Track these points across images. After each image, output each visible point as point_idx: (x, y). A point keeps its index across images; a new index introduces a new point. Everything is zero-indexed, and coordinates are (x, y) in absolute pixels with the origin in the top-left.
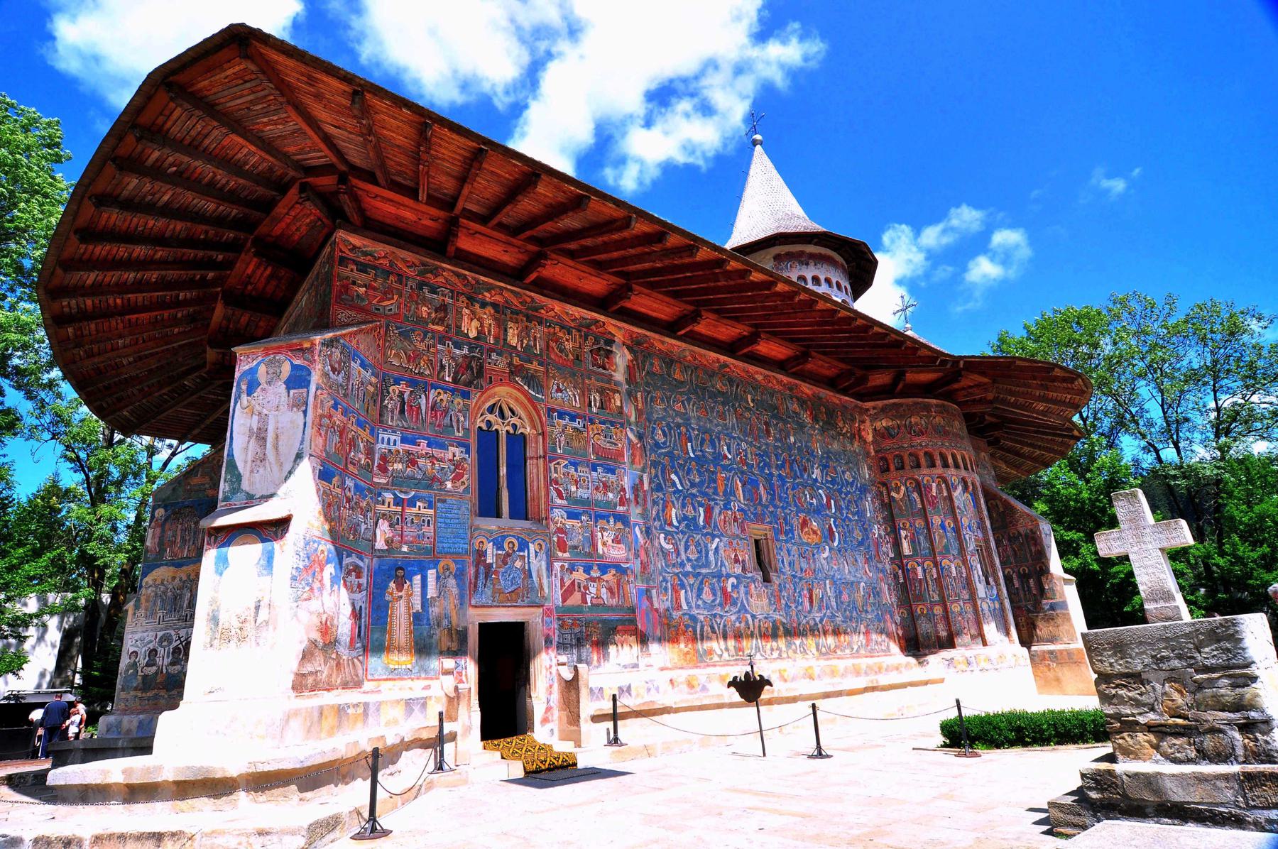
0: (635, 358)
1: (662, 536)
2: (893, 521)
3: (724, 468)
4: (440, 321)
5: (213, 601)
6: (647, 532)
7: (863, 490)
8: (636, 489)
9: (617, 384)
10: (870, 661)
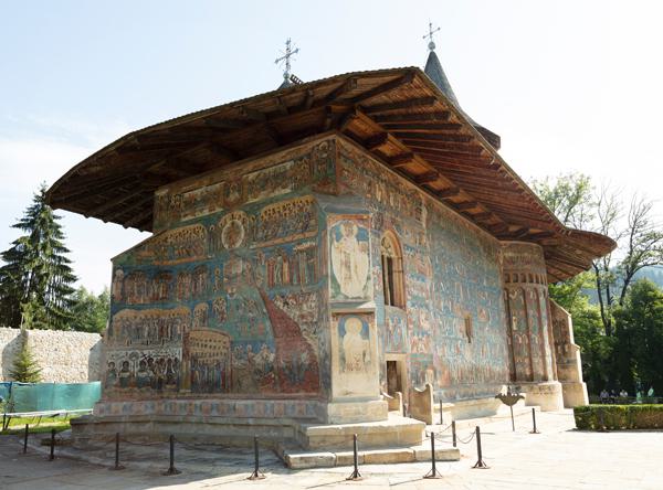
4: (369, 192)
5: (341, 350)
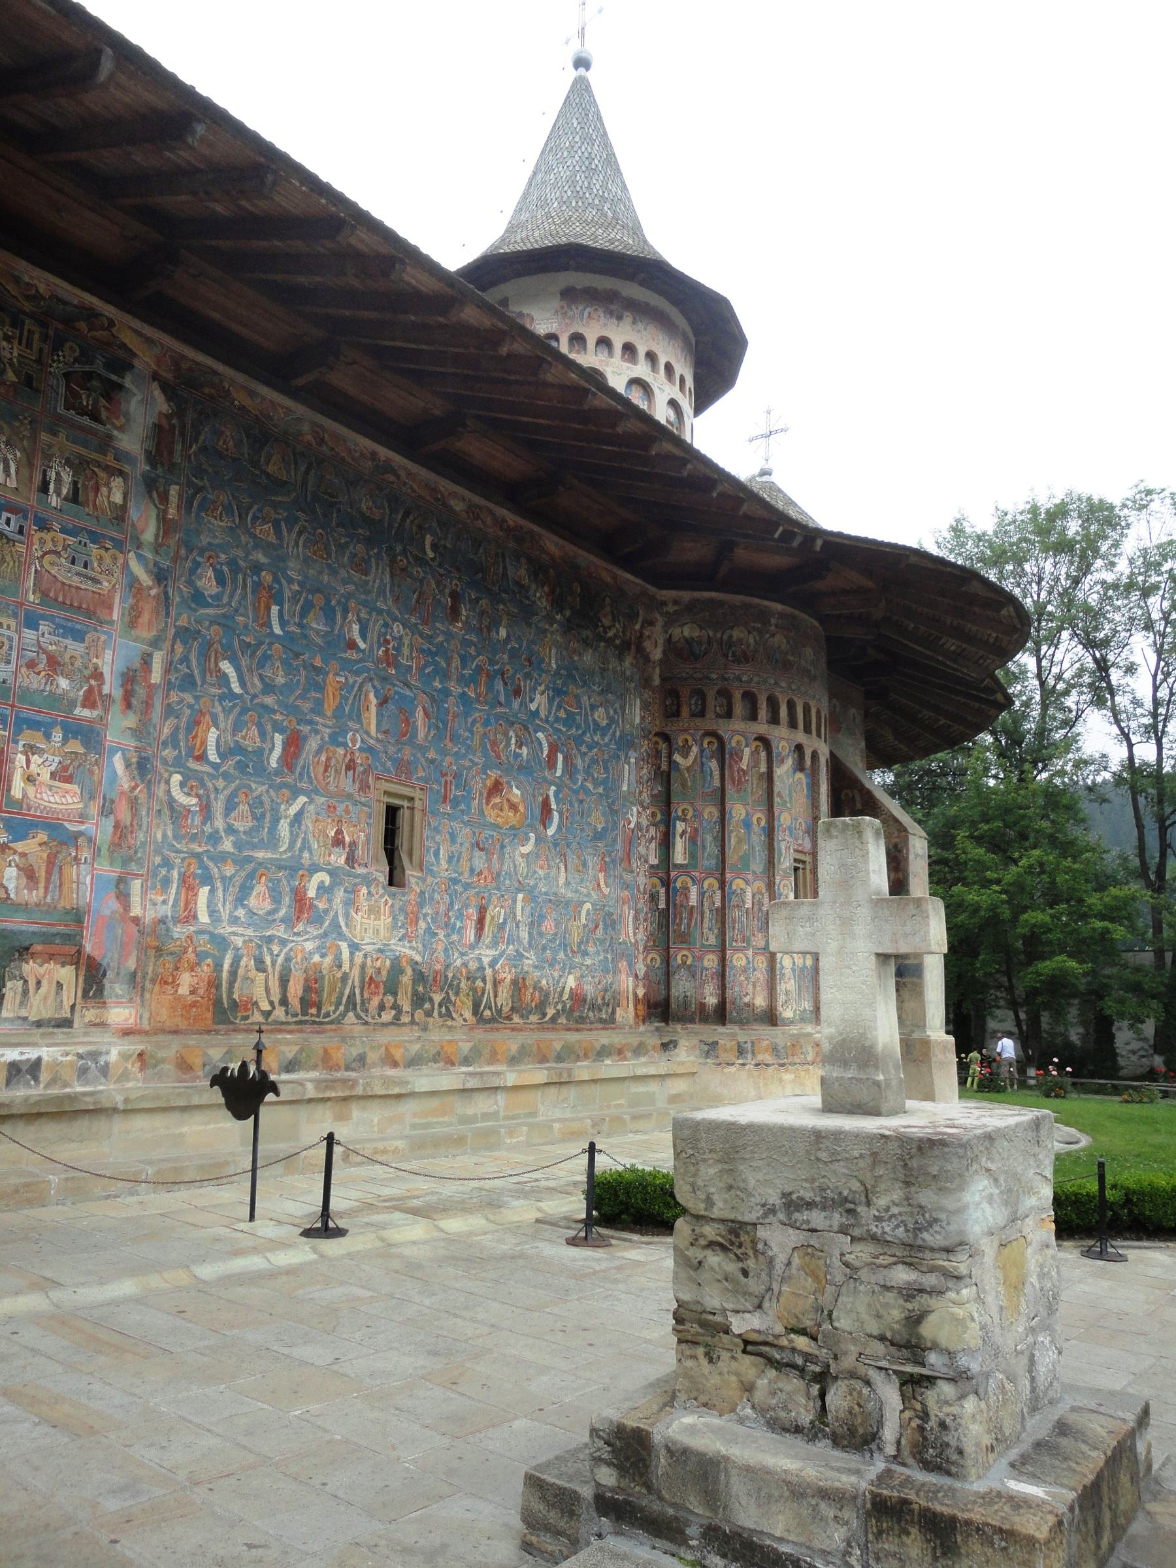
0: (180, 413)
1: (177, 778)
2: (668, 803)
3: (346, 665)
6: (142, 767)
7: (626, 743)
8: (129, 679)
9: (121, 456)
10: (573, 1037)
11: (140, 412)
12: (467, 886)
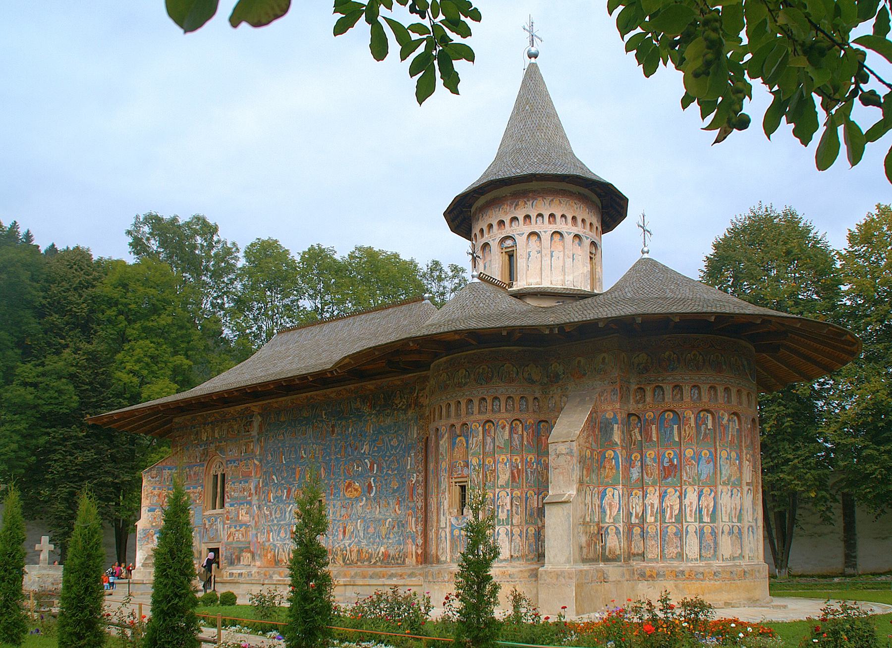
6: (259, 507)
8: (256, 488)
11: (257, 421)
12: (339, 521)
